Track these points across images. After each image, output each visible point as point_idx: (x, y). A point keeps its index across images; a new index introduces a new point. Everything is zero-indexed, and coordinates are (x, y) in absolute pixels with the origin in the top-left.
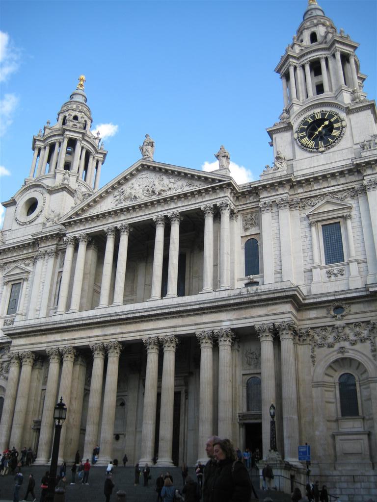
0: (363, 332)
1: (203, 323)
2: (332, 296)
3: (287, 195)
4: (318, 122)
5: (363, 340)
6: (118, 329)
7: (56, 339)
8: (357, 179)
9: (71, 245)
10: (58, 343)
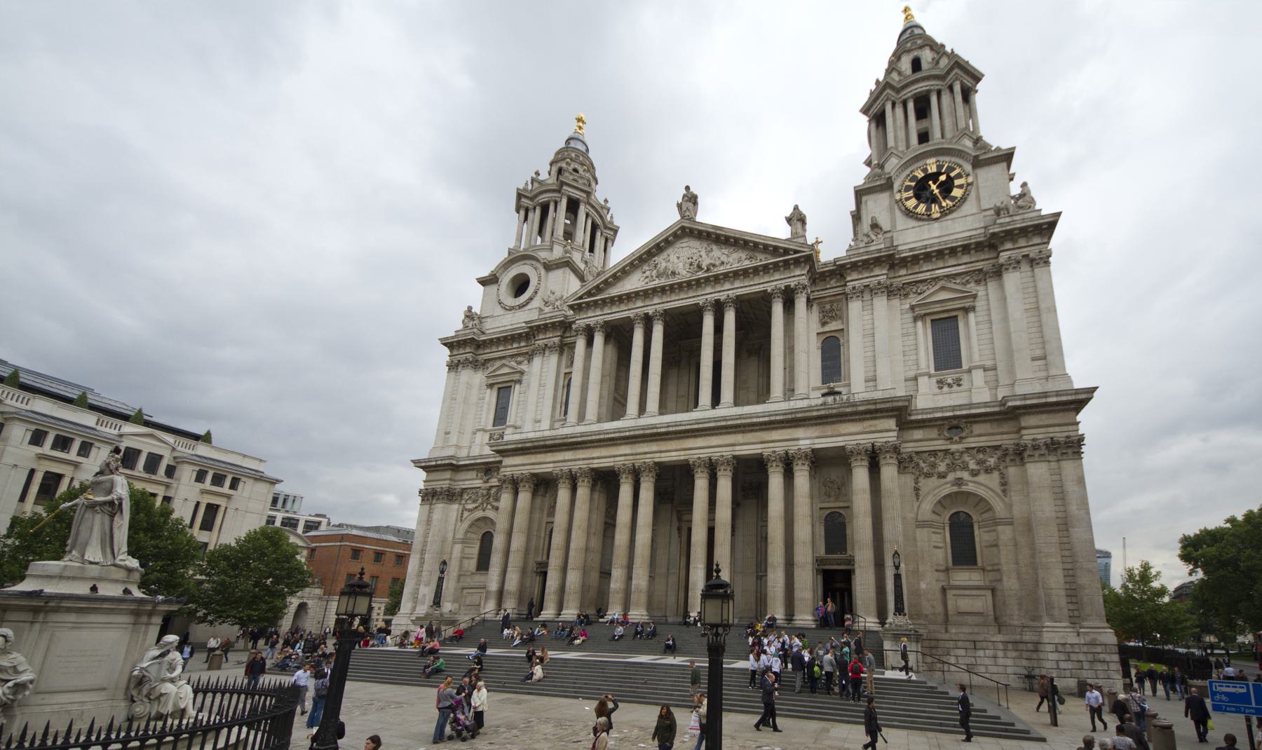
0: (989, 459)
1: (773, 441)
2: (949, 411)
3: (885, 277)
6: (654, 447)
7: (567, 458)
9: (583, 336)
10: (569, 463)
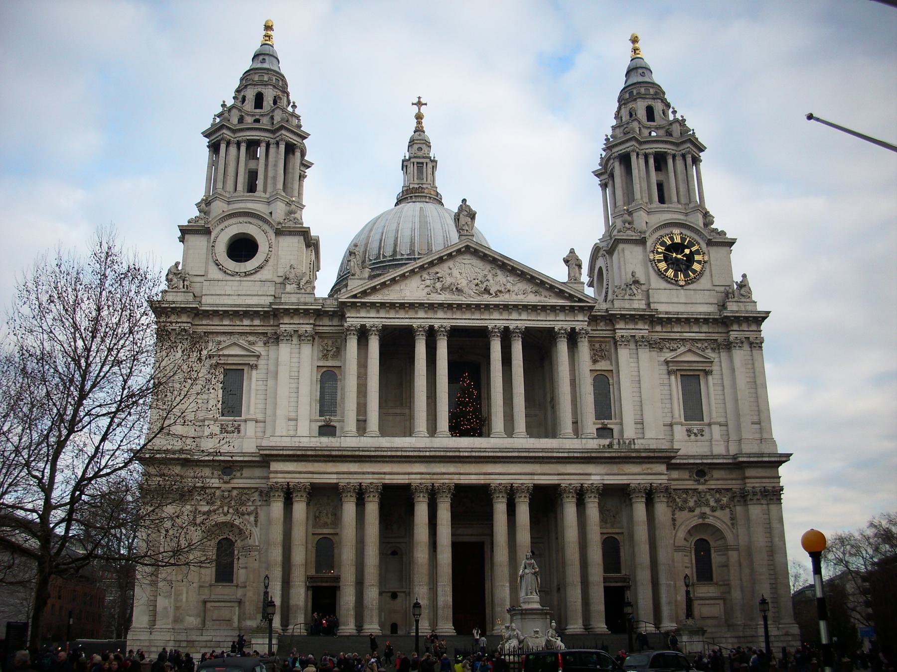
0: (723, 499)
2: (699, 459)
3: (647, 331)
4: (678, 248)
5: (722, 508)
6: (451, 468)
7: (352, 470)
8: (720, 331)
10: (355, 476)
